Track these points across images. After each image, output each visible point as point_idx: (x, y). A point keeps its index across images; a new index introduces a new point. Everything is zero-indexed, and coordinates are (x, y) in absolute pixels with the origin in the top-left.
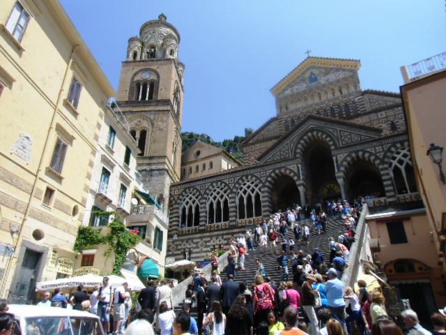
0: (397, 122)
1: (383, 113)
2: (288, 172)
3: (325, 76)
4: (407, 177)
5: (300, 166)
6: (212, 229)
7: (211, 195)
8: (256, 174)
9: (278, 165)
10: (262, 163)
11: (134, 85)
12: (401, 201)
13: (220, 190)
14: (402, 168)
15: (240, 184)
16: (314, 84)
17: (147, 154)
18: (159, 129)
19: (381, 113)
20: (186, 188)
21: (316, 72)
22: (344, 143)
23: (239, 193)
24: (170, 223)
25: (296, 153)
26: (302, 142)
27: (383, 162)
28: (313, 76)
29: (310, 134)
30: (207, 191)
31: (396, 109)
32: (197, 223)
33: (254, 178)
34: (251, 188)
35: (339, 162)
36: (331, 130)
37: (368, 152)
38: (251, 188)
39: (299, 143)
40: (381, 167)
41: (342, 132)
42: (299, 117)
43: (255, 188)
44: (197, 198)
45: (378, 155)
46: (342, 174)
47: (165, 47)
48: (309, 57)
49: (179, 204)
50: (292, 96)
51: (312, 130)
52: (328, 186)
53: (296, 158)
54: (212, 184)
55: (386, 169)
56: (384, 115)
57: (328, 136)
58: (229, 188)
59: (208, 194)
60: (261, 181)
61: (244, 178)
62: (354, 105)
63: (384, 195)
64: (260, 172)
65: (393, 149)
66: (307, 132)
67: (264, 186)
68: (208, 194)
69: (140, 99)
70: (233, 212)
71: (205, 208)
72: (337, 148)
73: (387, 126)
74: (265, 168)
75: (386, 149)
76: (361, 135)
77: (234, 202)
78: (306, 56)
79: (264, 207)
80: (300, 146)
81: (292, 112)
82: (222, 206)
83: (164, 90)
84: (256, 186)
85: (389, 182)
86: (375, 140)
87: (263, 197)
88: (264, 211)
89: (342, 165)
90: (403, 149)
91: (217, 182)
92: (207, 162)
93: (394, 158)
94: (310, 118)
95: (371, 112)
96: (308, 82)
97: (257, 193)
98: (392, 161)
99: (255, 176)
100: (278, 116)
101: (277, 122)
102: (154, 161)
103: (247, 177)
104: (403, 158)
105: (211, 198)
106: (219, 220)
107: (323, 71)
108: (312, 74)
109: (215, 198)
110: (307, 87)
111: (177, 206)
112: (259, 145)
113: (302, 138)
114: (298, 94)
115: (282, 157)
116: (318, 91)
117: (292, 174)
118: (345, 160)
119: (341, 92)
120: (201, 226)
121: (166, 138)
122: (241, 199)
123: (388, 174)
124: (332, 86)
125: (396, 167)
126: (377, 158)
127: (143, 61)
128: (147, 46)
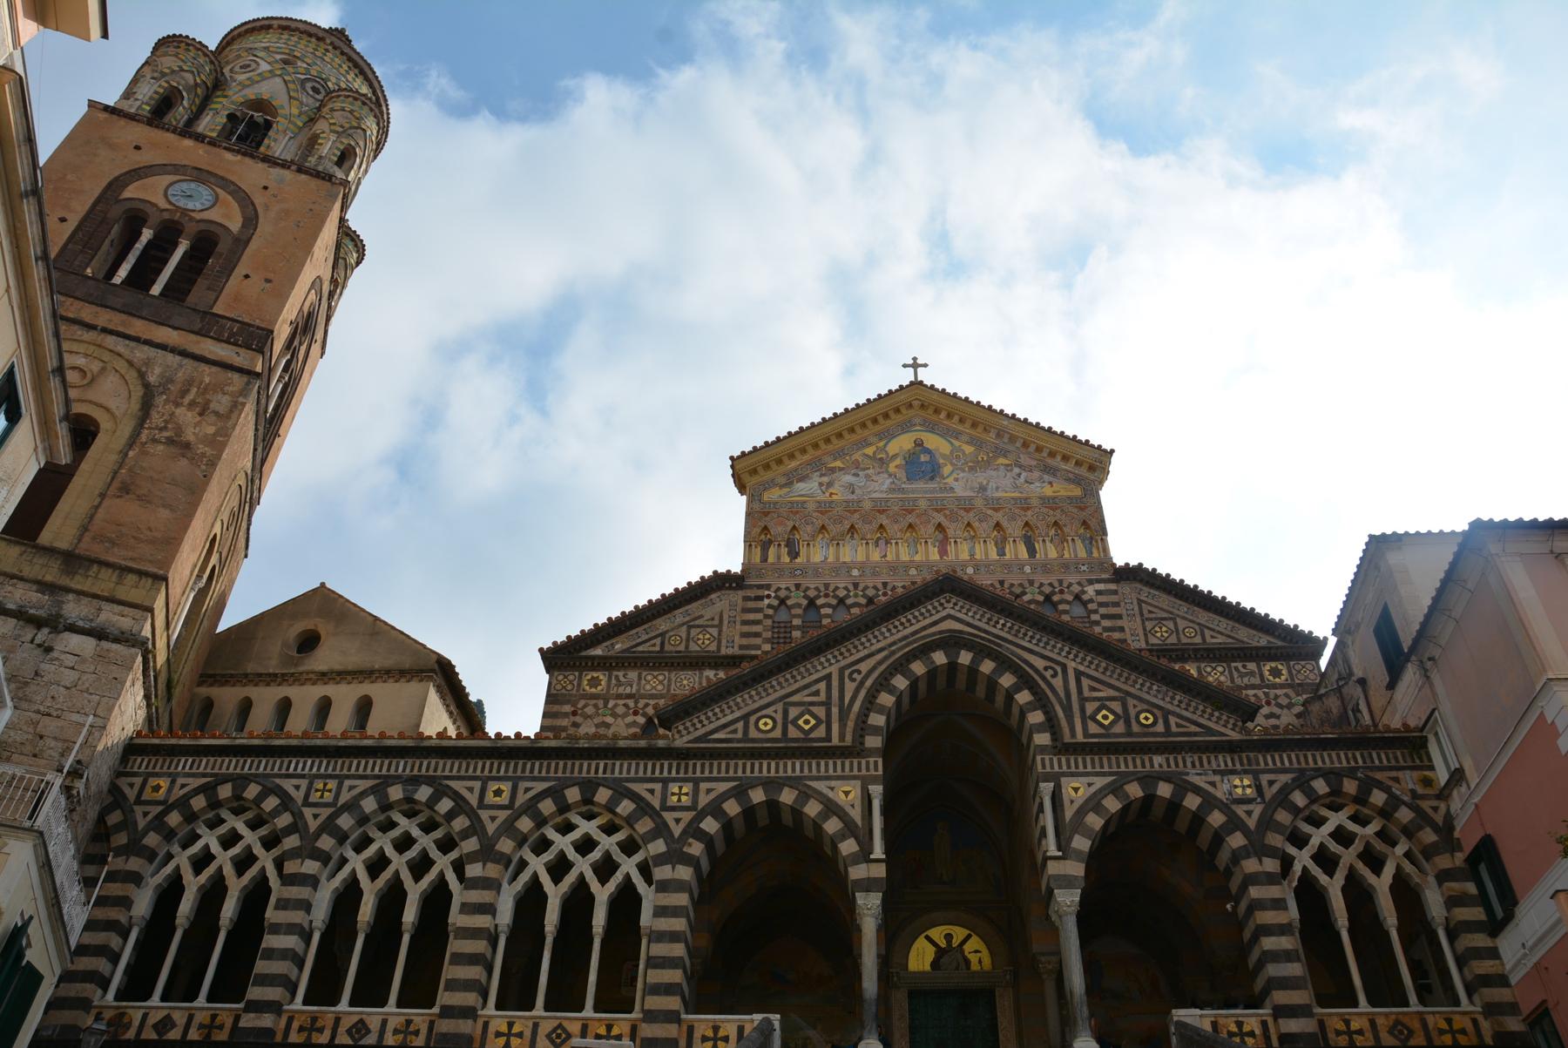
2: (812, 809)
3: (972, 469)
5: (877, 790)
7: (363, 844)
8: (639, 788)
9: (768, 769)
10: (681, 739)
11: (116, 211)
12: (1331, 1036)
13: (416, 832)
14: (1334, 887)
15: (541, 822)
16: (921, 489)
17: (59, 530)
18: (170, 441)
20: (224, 779)
22: (1093, 728)
23: (523, 864)
24: (90, 926)
25: (862, 728)
26: (901, 683)
27: (1263, 851)
28: (923, 458)
29: (940, 658)
30: (345, 822)
31: (1239, 665)
32: (230, 986)
33: (625, 807)
34: (596, 855)
35: (1069, 814)
36: (1040, 664)
37: (1197, 790)
38: (596, 855)
39: (883, 683)
40: (1250, 865)
41: (1085, 682)
42: (841, 601)
43: (618, 856)
44: (269, 843)
45: (1240, 810)
46: (1076, 869)
47: (321, 126)
48: (916, 384)
49: (150, 855)
50: (824, 508)
51: (952, 642)
52: (937, 933)
54: (379, 790)
55: (1271, 879)
57: (1026, 681)
58: (476, 828)
59: (342, 838)
60: (661, 830)
61: (573, 794)
62: (1078, 611)
63: (1254, 1003)
64: (665, 782)
65: (1299, 799)
67: (675, 856)
68: (342, 838)
69: (117, 280)
70: (473, 959)
71: (307, 906)
72: (1063, 748)
74: (698, 768)
75: (1269, 793)
76: (1166, 714)
77: (489, 909)
78: (906, 377)
79: (655, 963)
80: (886, 699)
81: (817, 571)
82: (410, 915)
83: (256, 282)
84: (629, 847)
85: (1286, 943)
86: (1232, 748)
87: (660, 912)
88: (656, 990)
89: (1078, 824)
90: (1336, 808)
91: (415, 781)
92: (345, 697)
93: (1300, 841)
94: (948, 585)
96: (902, 474)
97: (627, 887)
98: (1292, 850)
99: (635, 797)
100: (746, 566)
101: (737, 597)
102: (104, 582)
103: (589, 787)
104: (1334, 847)
105: (357, 863)
106: (370, 992)
107: (969, 449)
108: (919, 444)
109: (377, 866)
110: (891, 490)
111: (134, 864)
112: (633, 675)
113: (901, 667)
114: (851, 508)
115: (793, 733)
116: (939, 518)
117: (832, 826)
118: (1094, 804)
119: (1032, 551)
120: (257, 1007)
121: (195, 492)
122: (532, 899)
123: (1279, 904)
124: (998, 516)
126: (1235, 824)
127: (200, 138)
128: (239, 98)
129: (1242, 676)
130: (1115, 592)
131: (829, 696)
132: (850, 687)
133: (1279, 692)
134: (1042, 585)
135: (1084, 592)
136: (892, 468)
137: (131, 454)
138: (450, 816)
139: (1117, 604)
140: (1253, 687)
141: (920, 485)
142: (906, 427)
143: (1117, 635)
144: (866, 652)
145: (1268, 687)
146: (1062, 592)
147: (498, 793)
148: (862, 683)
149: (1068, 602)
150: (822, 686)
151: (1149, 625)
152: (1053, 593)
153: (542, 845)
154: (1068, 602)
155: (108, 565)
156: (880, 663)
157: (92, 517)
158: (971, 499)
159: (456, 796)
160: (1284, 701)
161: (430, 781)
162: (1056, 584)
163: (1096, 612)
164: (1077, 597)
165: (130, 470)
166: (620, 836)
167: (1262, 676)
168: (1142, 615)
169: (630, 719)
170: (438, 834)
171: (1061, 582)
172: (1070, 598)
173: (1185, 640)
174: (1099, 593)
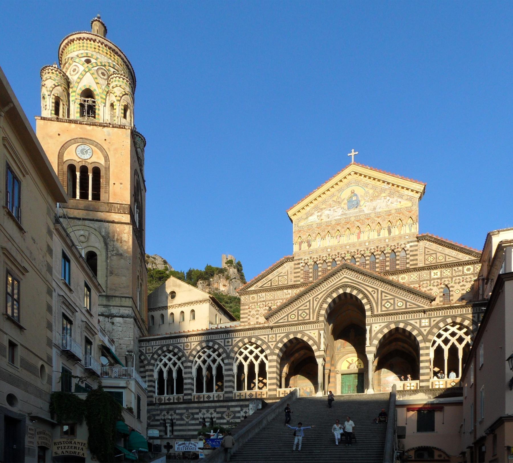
0: (452, 287)
1: (438, 271)
4: (448, 360)
6: (202, 400)
19: (435, 271)
21: (359, 191)
23: (237, 358)
28: (354, 198)
39: (324, 301)
53: (317, 322)
56: (439, 276)
62: (403, 254)
66: (338, 288)
73: (438, 291)
95: (422, 269)
108: (353, 192)
125: (439, 347)
129: (456, 272)
130: (417, 246)
131: (310, 307)
132: (315, 303)
133: (467, 277)
134: (391, 246)
135: (405, 247)
136: (342, 205)
137: (108, 261)
138: (218, 349)
139: (416, 250)
140: (459, 276)
141: (352, 211)
142: (348, 185)
143: (415, 262)
144: (320, 292)
145: (464, 275)
146: (398, 248)
147: (228, 342)
148: (319, 301)
149: (400, 252)
150: (308, 304)
151: (426, 257)
152: (395, 249)
153: (241, 353)
154: (400, 252)
155: (115, 297)
156: (324, 295)
157: (107, 283)
158: (370, 214)
159: (219, 344)
160: (468, 280)
161: (212, 341)
162: (396, 245)
163: (409, 254)
164: (403, 249)
165: (110, 267)
166: (260, 349)
167: (463, 271)
168: (425, 253)
169: (265, 308)
170: (217, 353)
171: (398, 244)
172: (400, 250)
173: (438, 261)
174: (411, 246)
